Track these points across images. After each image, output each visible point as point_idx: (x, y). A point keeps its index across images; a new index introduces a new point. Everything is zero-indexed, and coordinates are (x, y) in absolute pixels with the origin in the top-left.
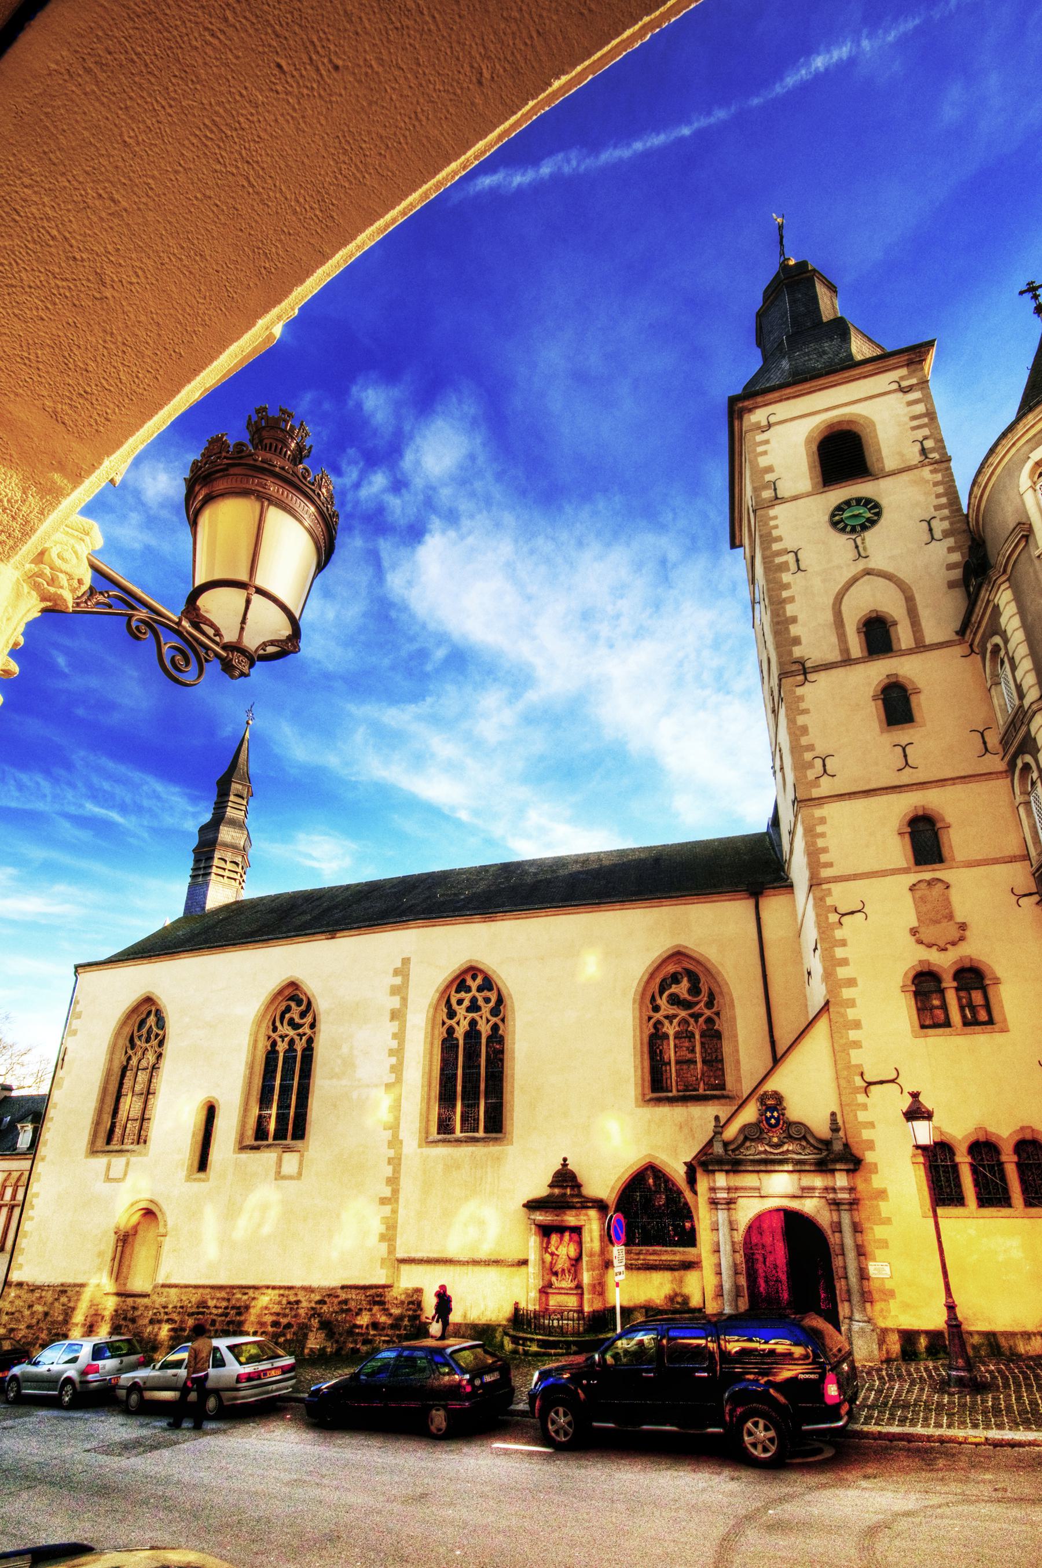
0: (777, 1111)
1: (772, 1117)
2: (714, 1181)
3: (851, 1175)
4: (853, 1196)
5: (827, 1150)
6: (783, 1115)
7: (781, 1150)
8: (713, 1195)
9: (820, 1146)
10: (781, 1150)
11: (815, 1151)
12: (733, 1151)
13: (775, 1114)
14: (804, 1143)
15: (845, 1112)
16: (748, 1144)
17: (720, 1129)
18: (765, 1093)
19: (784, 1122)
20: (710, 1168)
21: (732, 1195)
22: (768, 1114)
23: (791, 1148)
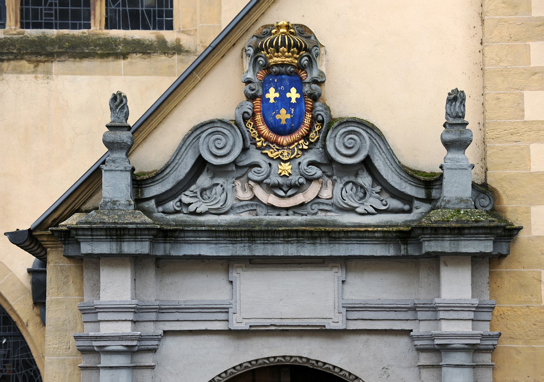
0: (299, 85)
1: (284, 101)
2: (96, 288)
3: (485, 272)
4: (484, 328)
5: (428, 200)
6: (315, 98)
7: (299, 199)
8: (90, 330)
9: (409, 189)
10: (299, 199)
11: (395, 204)
12: (161, 200)
13: (293, 95)
14: (365, 180)
15: (491, 93)
16: (204, 180)
17: (124, 136)
18: (267, 31)
19: (314, 119)
20: (86, 248)
21: (149, 329)
22: (272, 95)
23: (326, 194)
